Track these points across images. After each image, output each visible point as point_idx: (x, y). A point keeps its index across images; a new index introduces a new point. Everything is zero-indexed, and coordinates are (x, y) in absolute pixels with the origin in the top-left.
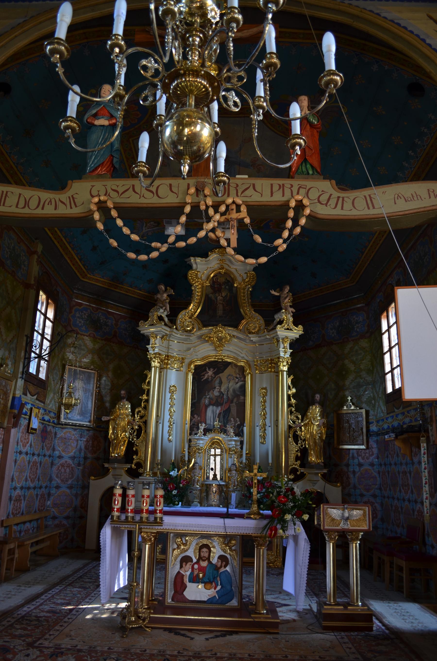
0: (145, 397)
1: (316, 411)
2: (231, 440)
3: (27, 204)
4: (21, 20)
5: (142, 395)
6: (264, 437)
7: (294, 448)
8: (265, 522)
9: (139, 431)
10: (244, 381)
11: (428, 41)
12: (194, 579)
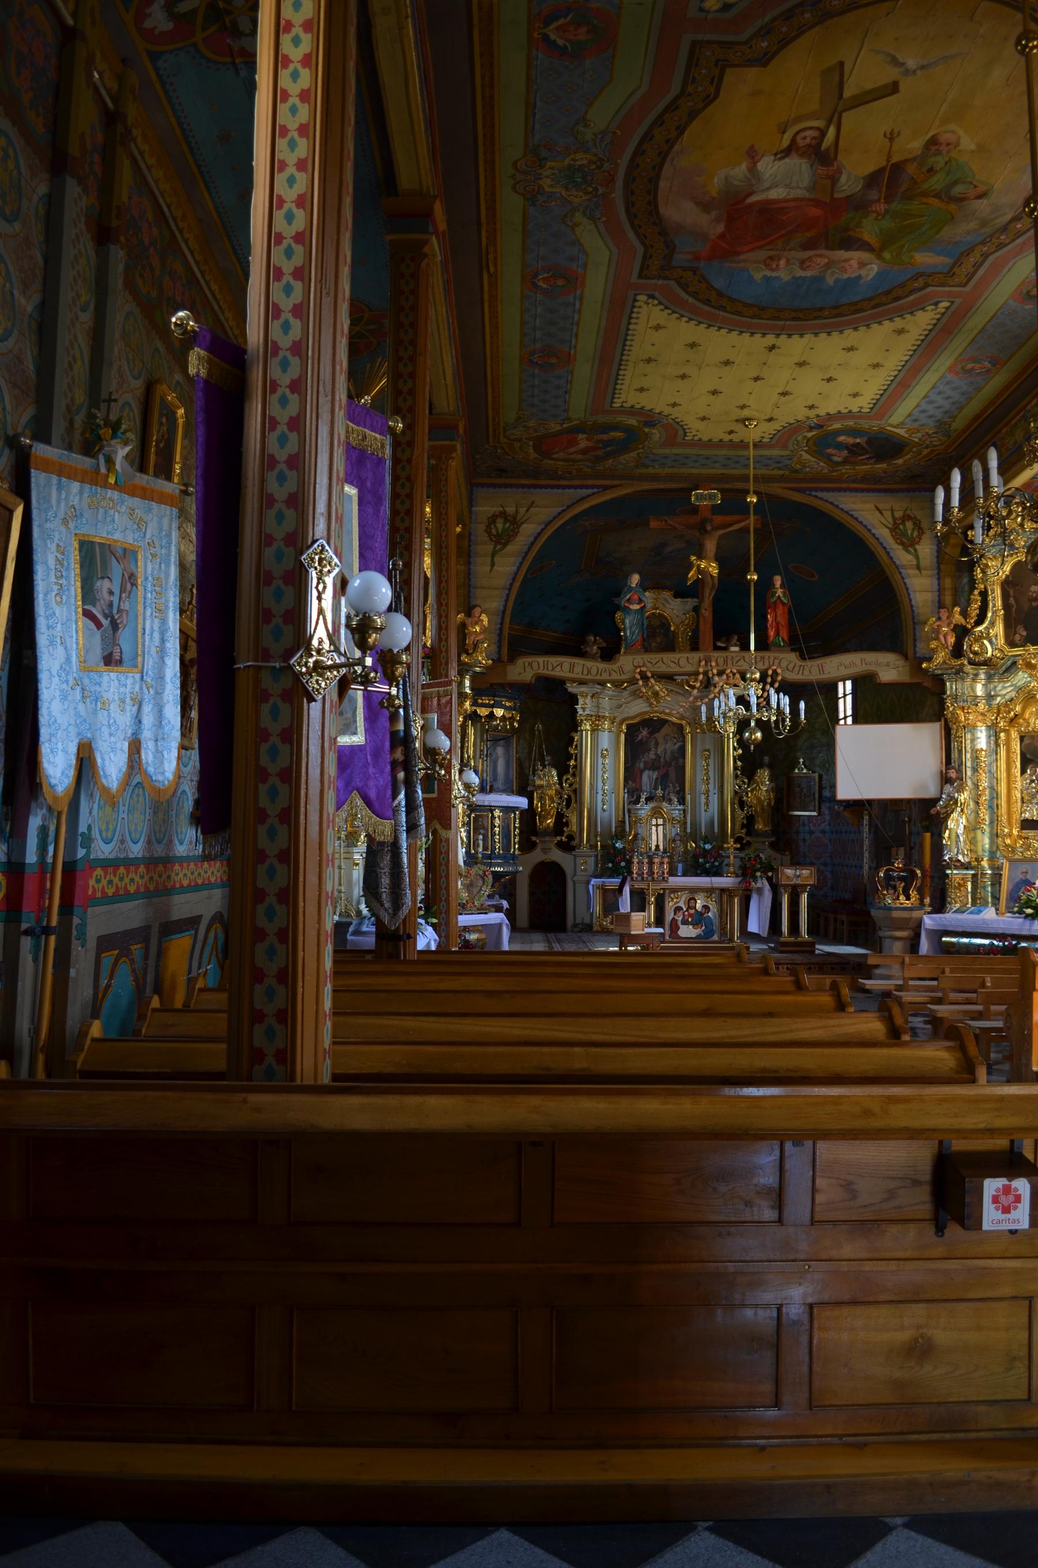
0: (572, 763)
1: (764, 776)
2: (674, 810)
3: (589, 672)
4: (560, 510)
5: (570, 760)
6: (707, 804)
7: (741, 815)
8: (740, 879)
9: (569, 801)
10: (684, 741)
11: (873, 531)
12: (685, 922)
